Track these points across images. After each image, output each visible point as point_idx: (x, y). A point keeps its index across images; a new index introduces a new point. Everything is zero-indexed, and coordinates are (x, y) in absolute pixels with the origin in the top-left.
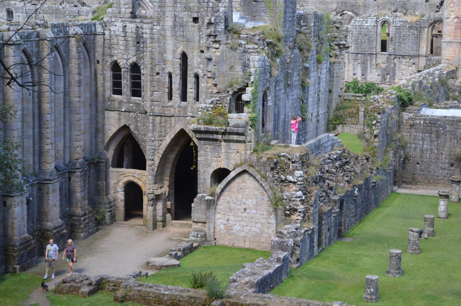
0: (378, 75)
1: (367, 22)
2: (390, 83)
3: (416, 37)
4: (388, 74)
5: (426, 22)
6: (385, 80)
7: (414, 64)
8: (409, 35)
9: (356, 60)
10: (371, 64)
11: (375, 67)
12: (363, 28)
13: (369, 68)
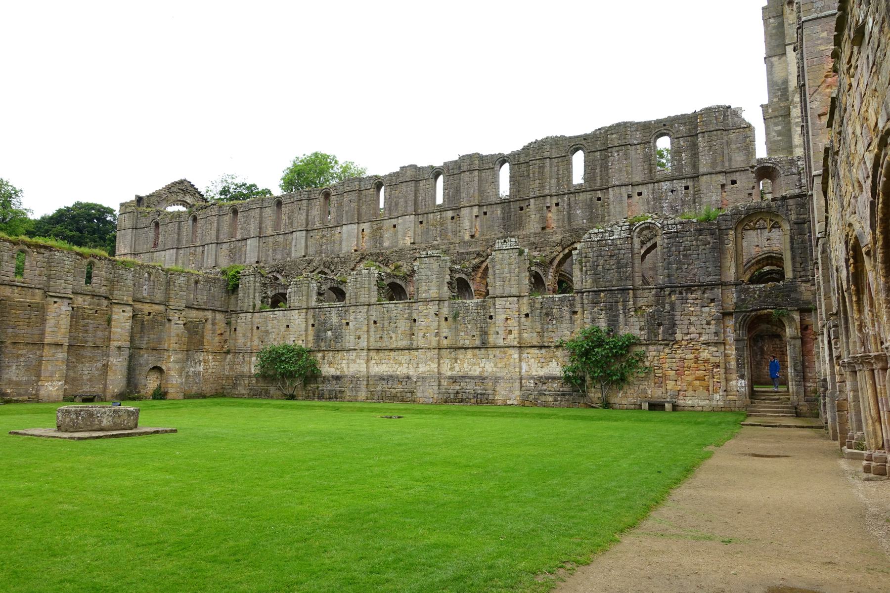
0: (641, 329)
1: (612, 233)
2: (665, 342)
3: (713, 248)
4: (659, 325)
5: (729, 218)
6: (656, 336)
7: (712, 300)
8: (698, 246)
9: (595, 303)
10: (625, 308)
11: (633, 313)
12: (606, 245)
13: (621, 316)
